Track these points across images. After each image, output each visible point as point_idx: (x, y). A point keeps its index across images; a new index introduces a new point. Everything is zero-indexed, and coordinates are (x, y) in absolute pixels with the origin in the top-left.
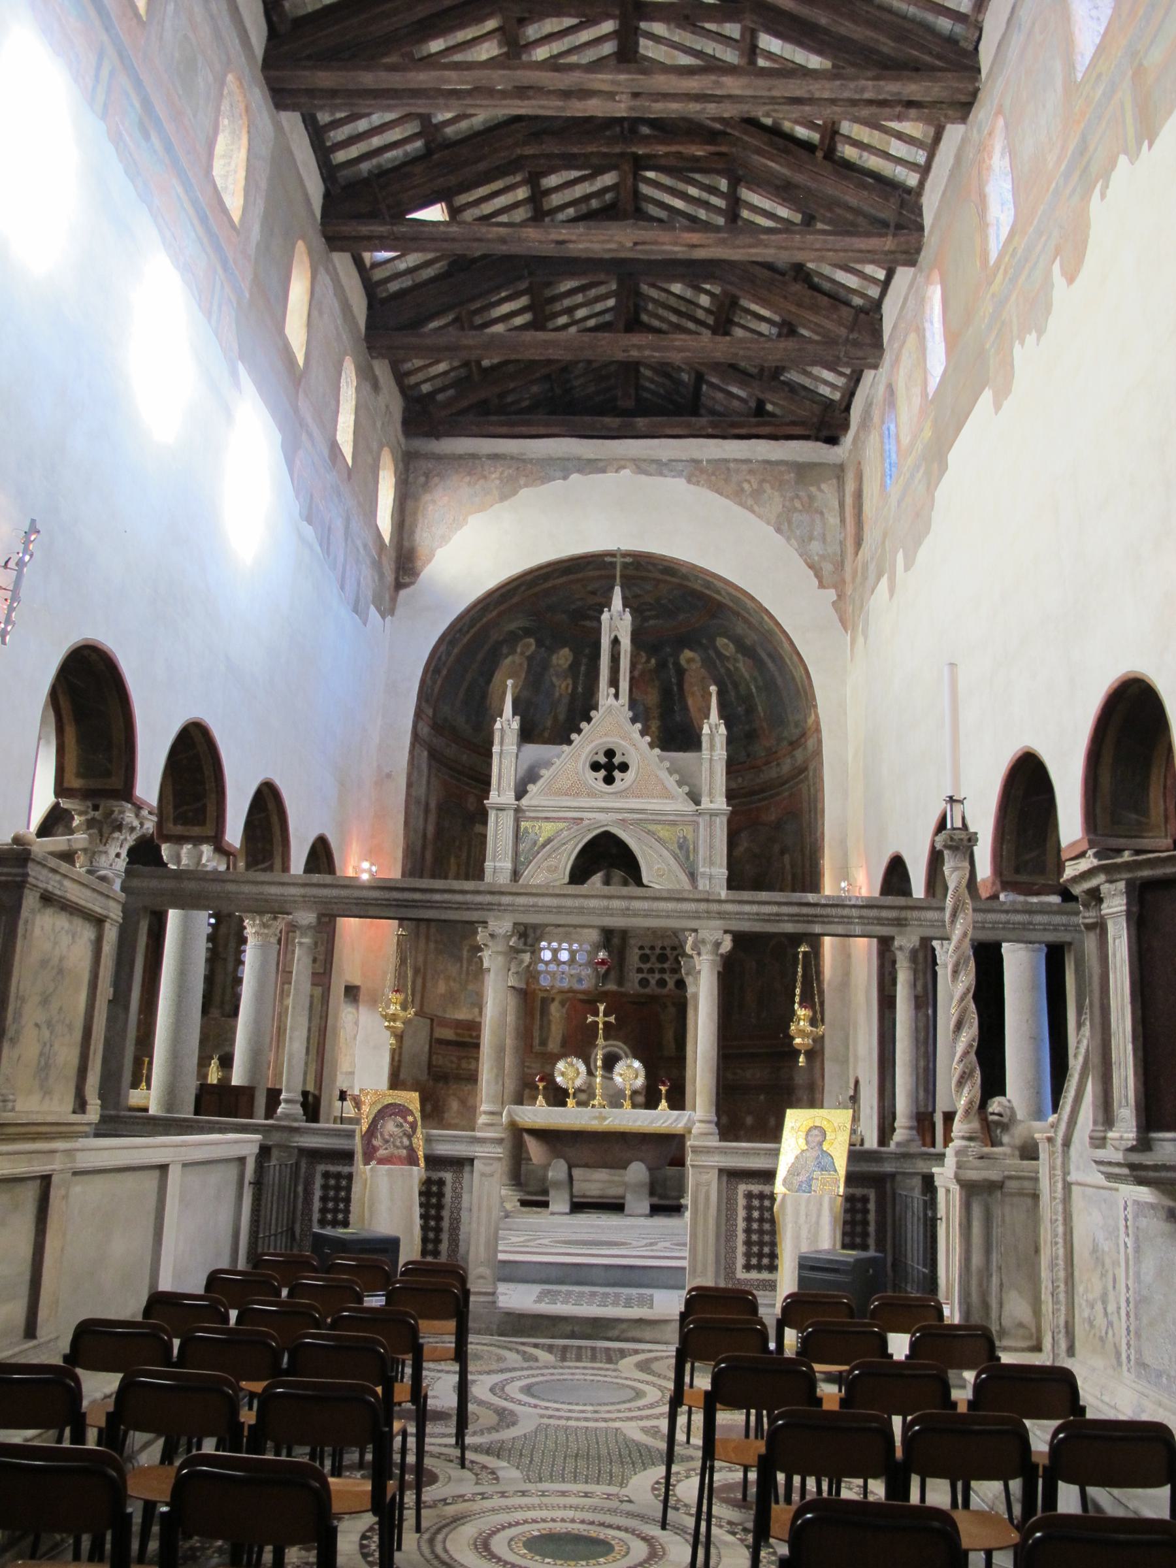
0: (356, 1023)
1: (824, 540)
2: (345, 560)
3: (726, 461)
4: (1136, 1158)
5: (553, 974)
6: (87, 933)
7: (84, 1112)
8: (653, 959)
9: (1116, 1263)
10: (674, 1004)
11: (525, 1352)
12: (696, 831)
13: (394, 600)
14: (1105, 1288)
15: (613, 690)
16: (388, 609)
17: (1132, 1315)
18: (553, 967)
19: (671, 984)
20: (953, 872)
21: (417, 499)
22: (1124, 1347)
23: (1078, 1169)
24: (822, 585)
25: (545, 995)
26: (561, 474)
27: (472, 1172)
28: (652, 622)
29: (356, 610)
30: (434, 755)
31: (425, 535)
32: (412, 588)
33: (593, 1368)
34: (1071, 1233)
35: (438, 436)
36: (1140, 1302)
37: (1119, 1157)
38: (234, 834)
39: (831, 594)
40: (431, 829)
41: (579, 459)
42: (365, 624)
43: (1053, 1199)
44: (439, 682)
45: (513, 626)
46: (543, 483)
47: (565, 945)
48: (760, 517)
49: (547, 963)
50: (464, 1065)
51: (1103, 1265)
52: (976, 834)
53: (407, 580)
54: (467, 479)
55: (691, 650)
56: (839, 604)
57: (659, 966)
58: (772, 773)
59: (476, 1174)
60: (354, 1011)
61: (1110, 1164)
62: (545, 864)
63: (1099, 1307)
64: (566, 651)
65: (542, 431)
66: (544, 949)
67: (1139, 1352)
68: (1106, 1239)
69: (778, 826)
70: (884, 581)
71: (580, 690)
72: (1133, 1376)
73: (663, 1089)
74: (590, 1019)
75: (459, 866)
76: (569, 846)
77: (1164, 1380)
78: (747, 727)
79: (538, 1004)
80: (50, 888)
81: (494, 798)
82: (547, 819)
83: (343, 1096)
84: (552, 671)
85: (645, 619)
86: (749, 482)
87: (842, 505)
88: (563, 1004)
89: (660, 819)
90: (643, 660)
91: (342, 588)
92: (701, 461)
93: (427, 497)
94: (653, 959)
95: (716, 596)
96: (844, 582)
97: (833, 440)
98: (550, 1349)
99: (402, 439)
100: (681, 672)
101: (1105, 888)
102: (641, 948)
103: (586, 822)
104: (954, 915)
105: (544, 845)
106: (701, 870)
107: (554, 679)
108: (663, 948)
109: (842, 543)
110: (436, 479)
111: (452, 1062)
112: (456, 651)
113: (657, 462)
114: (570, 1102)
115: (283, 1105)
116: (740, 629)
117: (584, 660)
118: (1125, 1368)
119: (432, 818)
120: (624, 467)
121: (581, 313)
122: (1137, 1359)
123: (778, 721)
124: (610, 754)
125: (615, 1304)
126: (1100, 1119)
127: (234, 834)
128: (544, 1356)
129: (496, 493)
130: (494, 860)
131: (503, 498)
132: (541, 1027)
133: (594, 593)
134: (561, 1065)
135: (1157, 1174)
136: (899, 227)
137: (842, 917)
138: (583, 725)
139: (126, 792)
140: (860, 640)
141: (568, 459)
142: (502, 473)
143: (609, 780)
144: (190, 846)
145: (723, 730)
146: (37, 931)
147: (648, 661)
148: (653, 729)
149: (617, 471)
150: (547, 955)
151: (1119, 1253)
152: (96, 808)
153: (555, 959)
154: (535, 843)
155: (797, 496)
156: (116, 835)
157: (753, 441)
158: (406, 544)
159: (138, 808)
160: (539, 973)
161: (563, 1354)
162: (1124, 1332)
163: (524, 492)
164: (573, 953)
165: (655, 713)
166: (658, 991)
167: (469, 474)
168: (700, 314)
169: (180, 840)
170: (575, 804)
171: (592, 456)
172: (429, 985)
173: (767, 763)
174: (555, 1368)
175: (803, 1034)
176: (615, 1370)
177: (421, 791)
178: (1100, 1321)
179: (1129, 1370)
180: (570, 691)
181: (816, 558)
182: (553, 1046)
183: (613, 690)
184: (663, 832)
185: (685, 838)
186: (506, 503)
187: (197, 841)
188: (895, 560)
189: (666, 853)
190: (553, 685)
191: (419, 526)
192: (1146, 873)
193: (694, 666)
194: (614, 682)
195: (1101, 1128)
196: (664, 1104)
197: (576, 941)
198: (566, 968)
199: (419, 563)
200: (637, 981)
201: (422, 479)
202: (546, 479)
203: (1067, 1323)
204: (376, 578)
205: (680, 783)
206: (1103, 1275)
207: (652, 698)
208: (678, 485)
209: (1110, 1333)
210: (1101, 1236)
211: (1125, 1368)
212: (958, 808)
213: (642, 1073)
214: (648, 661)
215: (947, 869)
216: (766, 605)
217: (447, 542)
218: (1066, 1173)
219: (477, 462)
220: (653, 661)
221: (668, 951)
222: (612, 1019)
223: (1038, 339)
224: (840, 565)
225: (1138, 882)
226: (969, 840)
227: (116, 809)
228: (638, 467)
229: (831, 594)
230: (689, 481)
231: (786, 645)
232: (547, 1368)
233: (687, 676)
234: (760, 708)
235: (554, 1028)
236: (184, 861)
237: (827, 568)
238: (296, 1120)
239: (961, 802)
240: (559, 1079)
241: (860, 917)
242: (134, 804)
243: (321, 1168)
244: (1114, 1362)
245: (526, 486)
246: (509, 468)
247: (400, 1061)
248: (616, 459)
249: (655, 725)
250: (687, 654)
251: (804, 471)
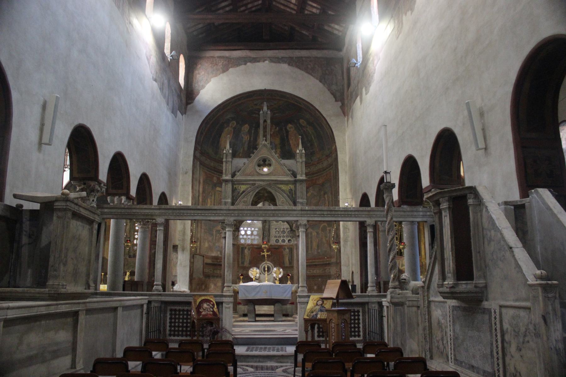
0: (177, 258)
2: (169, 95)
3: (302, 57)
4: (453, 290)
5: (245, 239)
6: (87, 227)
7: (89, 289)
8: (280, 233)
9: (446, 327)
10: (288, 248)
11: (243, 368)
12: (295, 187)
13: (186, 109)
14: (442, 335)
15: (265, 138)
16: (184, 112)
17: (452, 343)
18: (245, 237)
19: (287, 241)
20: (387, 197)
21: (193, 72)
22: (450, 354)
23: (432, 296)
24: (336, 101)
25: (243, 246)
26: (244, 63)
27: (222, 307)
28: (277, 115)
29: (173, 112)
30: (202, 164)
31: (196, 85)
32: (192, 104)
33: (267, 372)
34: (431, 318)
36: (456, 338)
37: (448, 290)
38: (133, 192)
39: (340, 104)
40: (201, 190)
41: (250, 57)
42: (176, 117)
43: (424, 307)
44: (202, 137)
45: (228, 117)
46: (237, 66)
47: (249, 229)
48: (314, 77)
49: (243, 235)
50: (215, 272)
51: (442, 328)
52: (394, 184)
53: (190, 102)
54: (211, 65)
55: (291, 124)
57: (282, 235)
58: (320, 166)
59: (224, 308)
60: (176, 254)
61: (444, 293)
62: (243, 200)
63: (441, 342)
64: (247, 126)
65: (236, 48)
66: (241, 230)
67: (455, 356)
68: (443, 319)
69: (323, 185)
70: (358, 98)
71: (252, 139)
72: (453, 364)
75: (211, 202)
76: (251, 193)
77: (464, 364)
78: (311, 151)
79: (240, 250)
80: (75, 211)
84: (242, 132)
86: (310, 65)
88: (249, 249)
89: (282, 182)
90: (274, 128)
91: (168, 104)
92: (293, 58)
93: (196, 72)
94: (280, 233)
95: (299, 105)
96: (343, 99)
98: (252, 367)
100: (287, 132)
101: (441, 200)
102: (276, 229)
103: (256, 185)
105: (242, 194)
106: (298, 200)
107: (243, 135)
108: (284, 229)
109: (343, 86)
110: (199, 66)
111: (211, 271)
112: (208, 126)
113: (278, 58)
115: (155, 286)
117: (253, 129)
118: (450, 361)
120: (266, 60)
121: (249, 6)
122: (454, 358)
124: (264, 160)
125: (273, 350)
126: (441, 278)
127: (133, 192)
128: (251, 370)
129: (221, 70)
131: (224, 72)
132: (242, 257)
133: (256, 105)
135: (461, 295)
137: (348, 215)
140: (350, 119)
141: (246, 58)
142: (223, 63)
144: (118, 197)
145: (304, 151)
146: (71, 226)
147: (276, 128)
148: (278, 152)
149: (264, 61)
150: (243, 232)
151: (447, 323)
152: (85, 184)
153: (246, 234)
154: (239, 193)
156: (92, 193)
157: (311, 51)
159: (100, 183)
160: (241, 238)
161: (257, 368)
162: (450, 350)
163: (231, 70)
164: (252, 232)
166: (282, 244)
167: (211, 63)
168: (292, 6)
169: (114, 195)
170: (253, 179)
171: (255, 57)
172: (202, 244)
173: (318, 163)
174: (254, 373)
176: (275, 373)
178: (441, 346)
179: (451, 362)
180: (248, 139)
181: (334, 91)
182: (246, 264)
183: (265, 138)
185: (291, 190)
186: (225, 74)
187: (120, 195)
188: (362, 91)
189: (285, 195)
190: (242, 137)
191: (194, 82)
192: (454, 194)
193: (292, 130)
194: (265, 136)
195: (441, 281)
197: (253, 227)
198: (249, 237)
200: (275, 240)
202: (238, 65)
203: (429, 349)
204: (179, 101)
206: (442, 331)
207: (277, 141)
208: (285, 67)
209: (445, 350)
210: (441, 318)
211: (450, 361)
212: (388, 175)
215: (385, 196)
216: (317, 107)
217: (204, 88)
218: (428, 298)
219: (214, 59)
220: (278, 128)
221: (285, 230)
223: (411, 13)
224: (342, 94)
225: (452, 197)
226: (392, 186)
227: (92, 184)
228: (270, 60)
229: (340, 104)
230: (289, 65)
232: (251, 373)
233: (290, 132)
234: (315, 144)
235: (246, 257)
236: (116, 202)
238: (160, 291)
239: (389, 173)
241: (354, 215)
242: (98, 182)
243: (169, 308)
244: (446, 360)
245: (231, 67)
246: (226, 61)
247: (193, 271)
248: (263, 57)
249: (279, 150)
250: (290, 125)
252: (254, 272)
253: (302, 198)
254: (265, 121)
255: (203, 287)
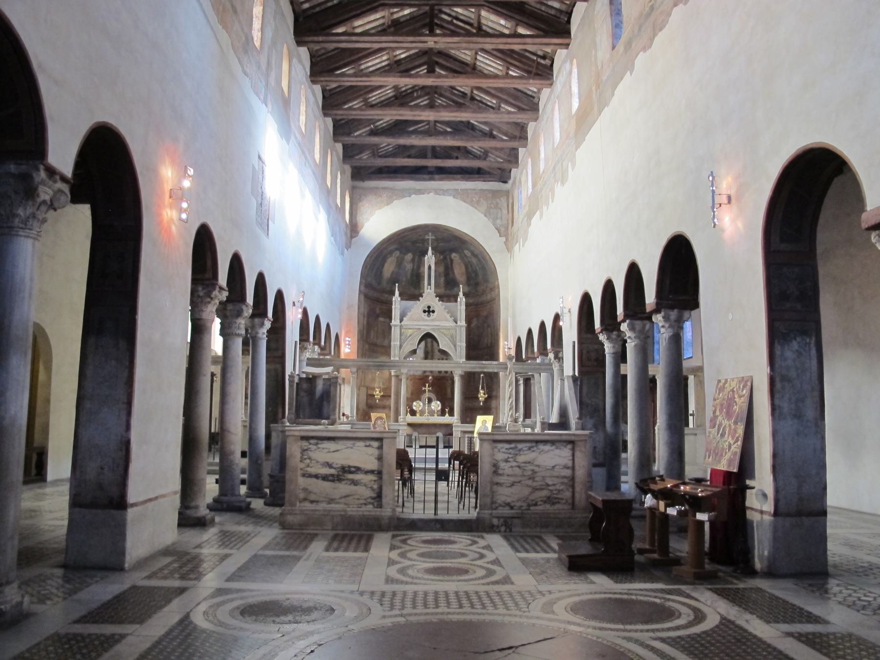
0: (344, 390)
1: (502, 219)
3: (467, 189)
12: (456, 331)
13: (350, 243)
24: (500, 236)
30: (366, 296)
31: (361, 218)
35: (363, 179)
38: (323, 343)
39: (504, 239)
45: (390, 249)
54: (375, 197)
56: (506, 243)
69: (487, 317)
70: (518, 244)
73: (447, 410)
74: (423, 389)
81: (393, 322)
82: (410, 329)
83: (344, 415)
85: (438, 243)
87: (508, 206)
92: (457, 190)
93: (361, 204)
96: (508, 234)
97: (505, 182)
99: (351, 182)
100: (452, 261)
104: (509, 374)
107: (406, 264)
109: (508, 220)
114: (418, 415)
116: (472, 248)
117: (417, 257)
119: (366, 319)
123: (486, 281)
124: (429, 307)
127: (323, 343)
130: (394, 341)
131: (388, 204)
134: (415, 403)
136: (520, 138)
138: (420, 298)
139: (308, 340)
143: (429, 315)
145: (464, 300)
147: (440, 257)
149: (428, 194)
154: (406, 336)
155: (492, 203)
158: (354, 221)
163: (395, 202)
165: (443, 275)
167: (375, 195)
173: (483, 294)
175: (482, 397)
177: (362, 310)
183: (429, 287)
184: (446, 332)
186: (389, 206)
194: (429, 284)
196: (447, 415)
199: (359, 229)
201: (358, 197)
202: (404, 197)
205: (451, 317)
208: (450, 199)
213: (440, 405)
214: (440, 257)
222: (430, 388)
224: (507, 228)
229: (504, 239)
230: (454, 197)
231: (488, 257)
237: (502, 229)
240: (414, 408)
245: (396, 199)
250: (454, 255)
251: (495, 194)
252: (417, 405)
253: (461, 341)
254: (430, 268)
255: (367, 418)
